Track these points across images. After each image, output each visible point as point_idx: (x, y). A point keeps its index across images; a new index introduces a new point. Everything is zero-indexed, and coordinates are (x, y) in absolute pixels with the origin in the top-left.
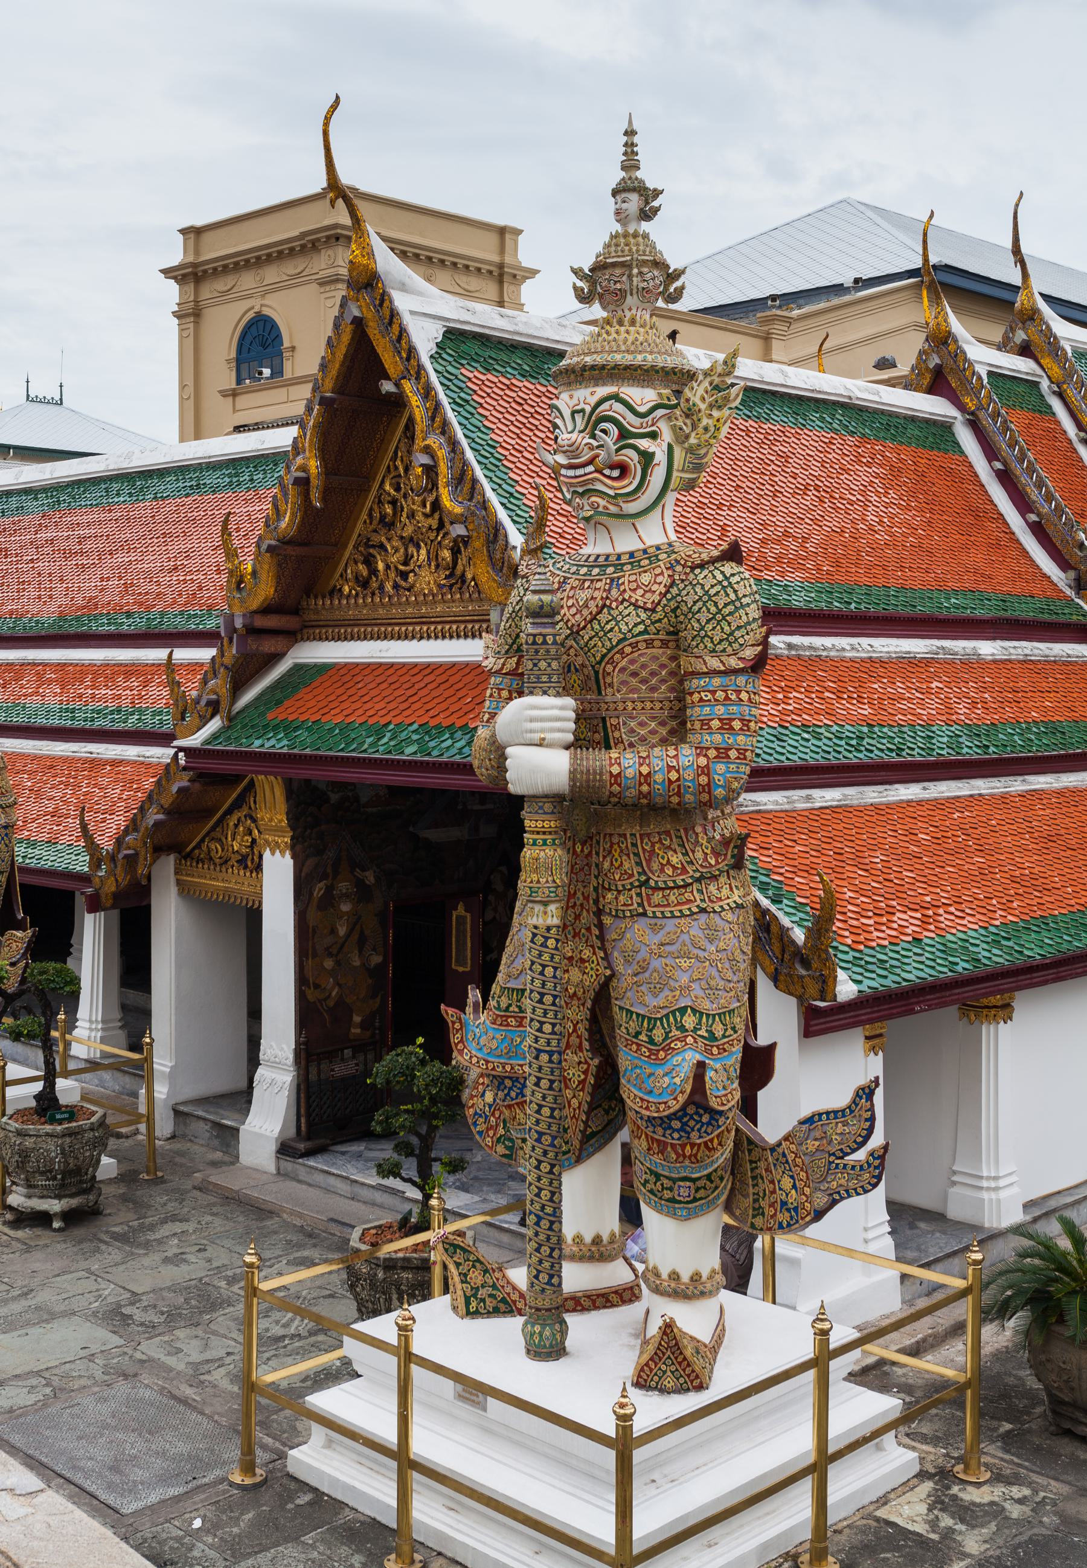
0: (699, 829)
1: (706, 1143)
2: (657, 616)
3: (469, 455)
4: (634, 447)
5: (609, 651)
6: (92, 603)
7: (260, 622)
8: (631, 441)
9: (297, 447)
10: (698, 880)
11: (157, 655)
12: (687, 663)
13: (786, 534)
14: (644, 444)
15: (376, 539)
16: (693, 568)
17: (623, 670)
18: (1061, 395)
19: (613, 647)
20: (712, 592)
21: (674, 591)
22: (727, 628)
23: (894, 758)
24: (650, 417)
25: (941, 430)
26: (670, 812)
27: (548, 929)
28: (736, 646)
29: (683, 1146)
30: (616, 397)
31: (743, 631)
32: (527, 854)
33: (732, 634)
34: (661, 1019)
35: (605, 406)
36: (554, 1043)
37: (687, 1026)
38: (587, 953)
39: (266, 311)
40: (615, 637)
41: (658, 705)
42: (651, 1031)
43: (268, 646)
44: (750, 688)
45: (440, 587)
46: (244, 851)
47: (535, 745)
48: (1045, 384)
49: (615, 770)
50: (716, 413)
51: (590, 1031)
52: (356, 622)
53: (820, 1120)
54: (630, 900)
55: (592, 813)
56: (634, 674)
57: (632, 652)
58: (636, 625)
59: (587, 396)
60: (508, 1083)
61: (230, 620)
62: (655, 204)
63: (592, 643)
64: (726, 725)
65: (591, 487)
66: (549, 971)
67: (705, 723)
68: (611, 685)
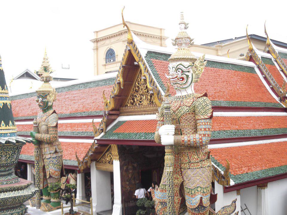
0: (200, 151)
1: (203, 213)
2: (190, 108)
3: (153, 77)
4: (185, 74)
5: (181, 115)
6: (77, 110)
7: (111, 113)
8: (184, 73)
9: (118, 77)
10: (201, 161)
11: (90, 121)
12: (197, 117)
13: (220, 91)
14: (187, 73)
15: (135, 94)
16: (197, 98)
17: (184, 119)
18: (276, 61)
19: (182, 114)
20: (202, 103)
21: (194, 103)
22: (205, 110)
23: (243, 137)
24: (188, 68)
25: (251, 69)
26: (195, 147)
27: (170, 172)
28: (206, 113)
30: (181, 64)
31: (208, 111)
32: (166, 157)
33: (206, 111)
35: (179, 66)
36: (172, 195)
37: (199, 190)
38: (179, 177)
39: (112, 48)
40: (182, 112)
41: (191, 126)
43: (113, 117)
44: (210, 122)
45: (148, 104)
46: (109, 160)
47: (166, 135)
48: (273, 59)
49: (183, 139)
50: (201, 67)
51: (179, 192)
52: (131, 112)
54: (187, 166)
55: (180, 149)
56: (186, 120)
58: (186, 110)
59: (175, 64)
60: (164, 203)
61: (105, 112)
62: (188, 26)
63: (178, 114)
64: (205, 129)
65: (176, 82)
66: (171, 180)
67: (201, 129)
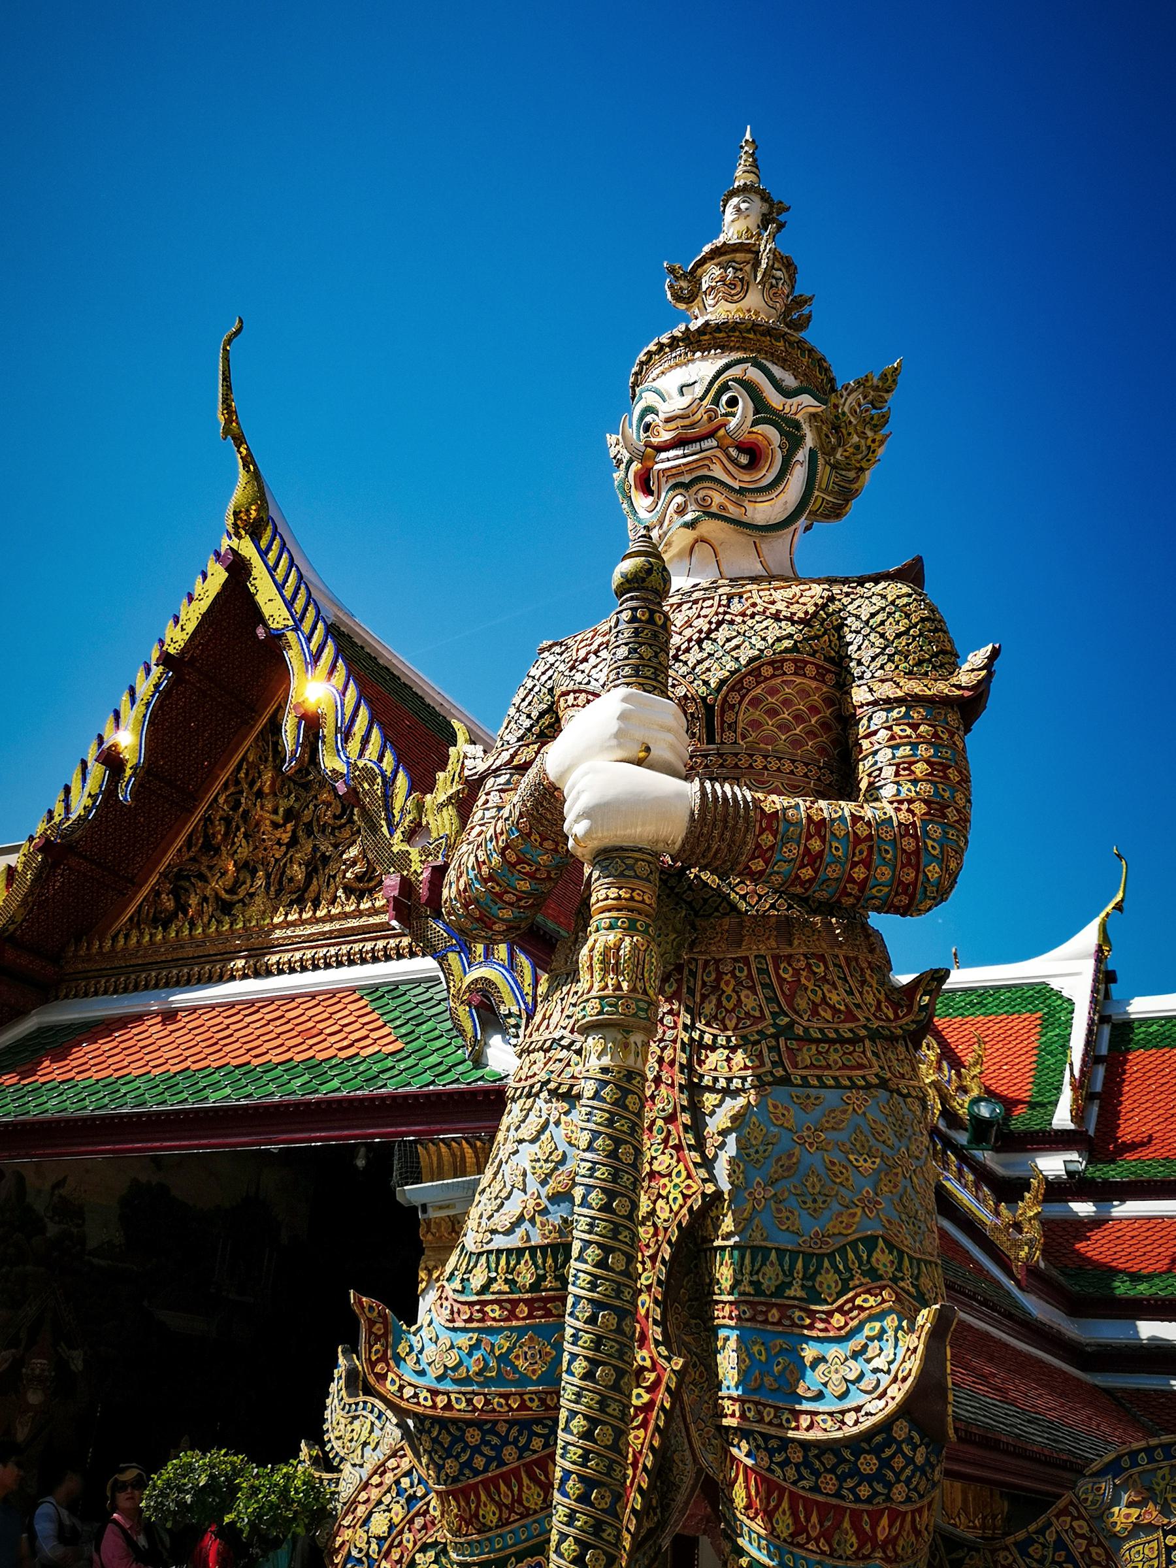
29: (875, 1519)
34: (831, 1256)
41: (801, 770)
42: (812, 1278)
53: (1135, 1464)
56: (772, 712)
57: (773, 676)
65: (705, 472)
68: (733, 727)
